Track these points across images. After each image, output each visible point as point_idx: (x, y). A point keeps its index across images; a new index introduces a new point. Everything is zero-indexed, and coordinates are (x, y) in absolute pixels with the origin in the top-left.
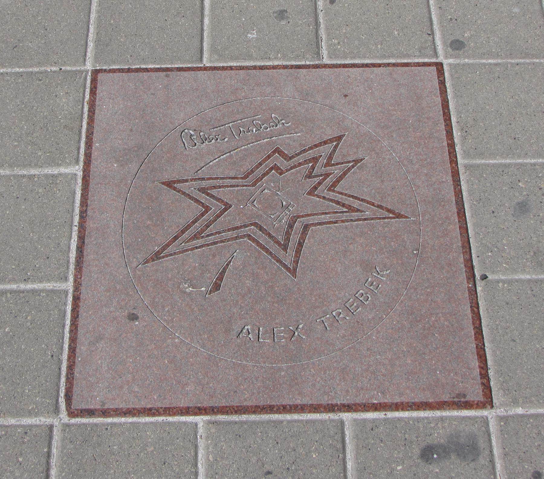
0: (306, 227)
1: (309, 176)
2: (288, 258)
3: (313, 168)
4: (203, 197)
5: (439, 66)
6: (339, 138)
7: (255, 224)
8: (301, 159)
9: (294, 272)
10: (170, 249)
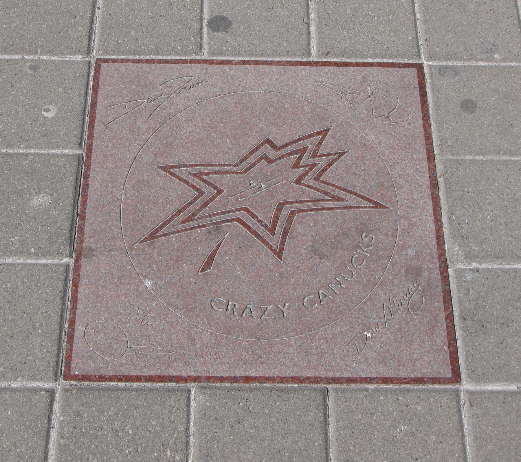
0: (293, 213)
1: (296, 165)
2: (275, 241)
3: (300, 158)
5: (420, 67)
7: (247, 210)
8: (289, 149)
9: (279, 254)
10: (165, 230)
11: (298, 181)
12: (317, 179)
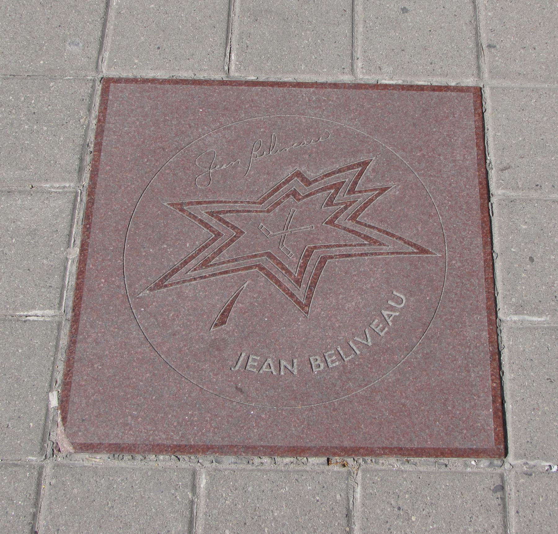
1: (330, 203)
4: (213, 222)
6: (366, 164)
7: (270, 255)
11: (331, 222)
12: (353, 218)
